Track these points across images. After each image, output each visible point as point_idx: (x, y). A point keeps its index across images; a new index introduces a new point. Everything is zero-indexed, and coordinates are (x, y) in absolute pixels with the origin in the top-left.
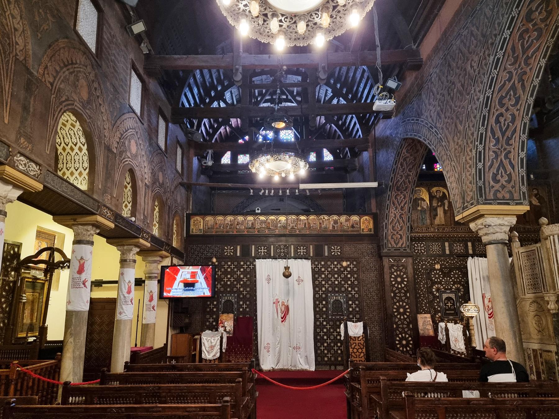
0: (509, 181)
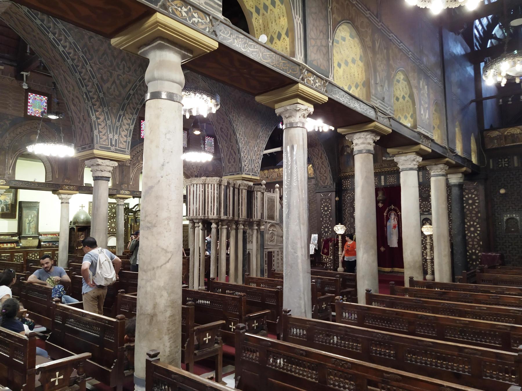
0: (234, 162)
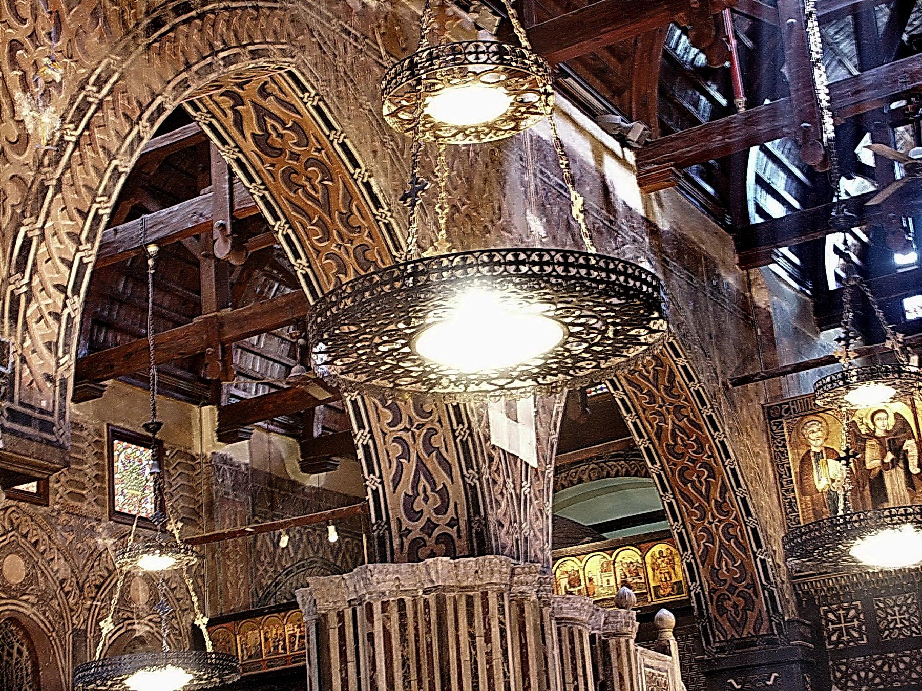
0: (441, 510)
